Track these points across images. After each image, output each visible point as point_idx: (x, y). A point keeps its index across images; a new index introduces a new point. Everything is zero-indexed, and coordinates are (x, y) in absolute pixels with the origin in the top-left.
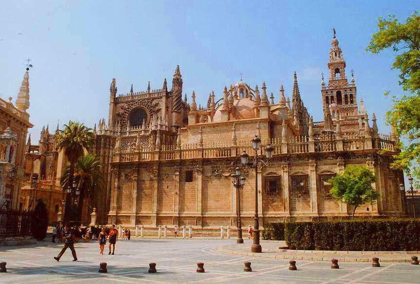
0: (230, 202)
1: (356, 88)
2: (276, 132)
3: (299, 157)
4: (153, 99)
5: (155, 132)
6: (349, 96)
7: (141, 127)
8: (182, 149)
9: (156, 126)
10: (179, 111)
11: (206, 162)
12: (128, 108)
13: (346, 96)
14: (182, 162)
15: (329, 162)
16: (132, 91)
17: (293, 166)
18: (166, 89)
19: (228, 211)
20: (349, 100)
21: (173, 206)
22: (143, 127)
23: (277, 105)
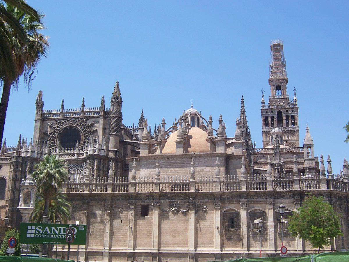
0: (188, 238)
1: (298, 108)
2: (231, 167)
3: (257, 194)
4: (88, 118)
5: (91, 157)
6: (290, 118)
7: (74, 149)
8: (137, 181)
9: (94, 151)
10: (118, 134)
11: (163, 196)
12: (58, 127)
13: (287, 117)
14: (138, 196)
15: (287, 200)
16: (63, 107)
17: (251, 203)
18: (104, 108)
19: (186, 247)
20: (290, 121)
21: (128, 242)
22: (76, 150)
23: (232, 139)
